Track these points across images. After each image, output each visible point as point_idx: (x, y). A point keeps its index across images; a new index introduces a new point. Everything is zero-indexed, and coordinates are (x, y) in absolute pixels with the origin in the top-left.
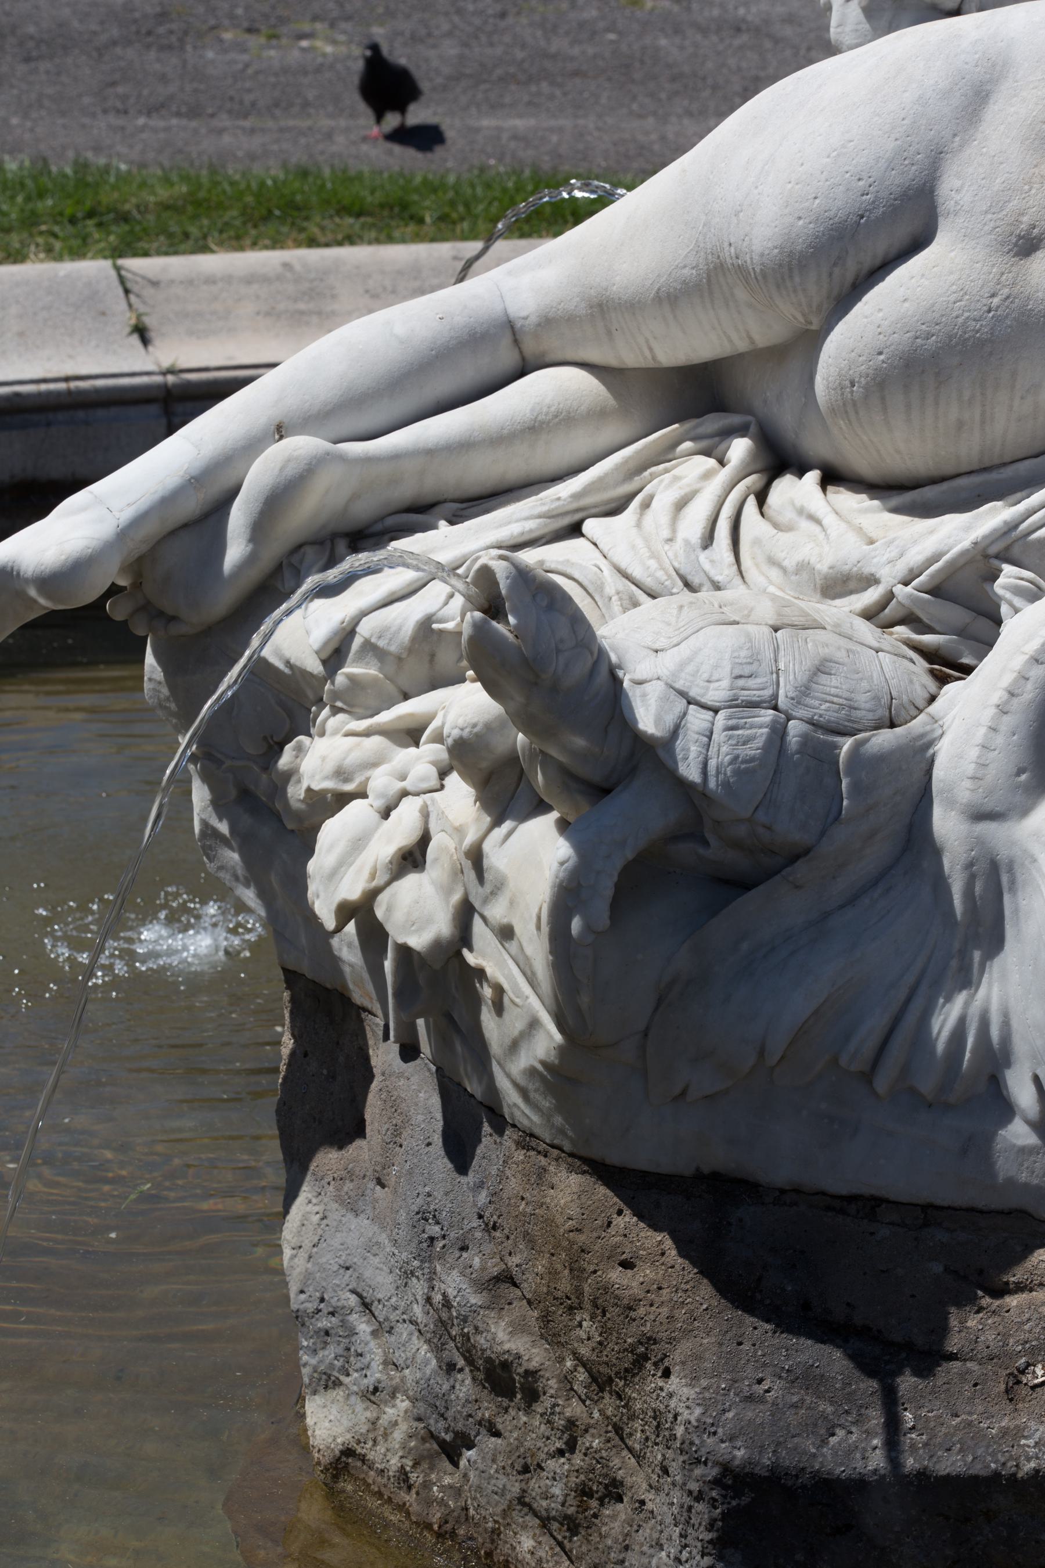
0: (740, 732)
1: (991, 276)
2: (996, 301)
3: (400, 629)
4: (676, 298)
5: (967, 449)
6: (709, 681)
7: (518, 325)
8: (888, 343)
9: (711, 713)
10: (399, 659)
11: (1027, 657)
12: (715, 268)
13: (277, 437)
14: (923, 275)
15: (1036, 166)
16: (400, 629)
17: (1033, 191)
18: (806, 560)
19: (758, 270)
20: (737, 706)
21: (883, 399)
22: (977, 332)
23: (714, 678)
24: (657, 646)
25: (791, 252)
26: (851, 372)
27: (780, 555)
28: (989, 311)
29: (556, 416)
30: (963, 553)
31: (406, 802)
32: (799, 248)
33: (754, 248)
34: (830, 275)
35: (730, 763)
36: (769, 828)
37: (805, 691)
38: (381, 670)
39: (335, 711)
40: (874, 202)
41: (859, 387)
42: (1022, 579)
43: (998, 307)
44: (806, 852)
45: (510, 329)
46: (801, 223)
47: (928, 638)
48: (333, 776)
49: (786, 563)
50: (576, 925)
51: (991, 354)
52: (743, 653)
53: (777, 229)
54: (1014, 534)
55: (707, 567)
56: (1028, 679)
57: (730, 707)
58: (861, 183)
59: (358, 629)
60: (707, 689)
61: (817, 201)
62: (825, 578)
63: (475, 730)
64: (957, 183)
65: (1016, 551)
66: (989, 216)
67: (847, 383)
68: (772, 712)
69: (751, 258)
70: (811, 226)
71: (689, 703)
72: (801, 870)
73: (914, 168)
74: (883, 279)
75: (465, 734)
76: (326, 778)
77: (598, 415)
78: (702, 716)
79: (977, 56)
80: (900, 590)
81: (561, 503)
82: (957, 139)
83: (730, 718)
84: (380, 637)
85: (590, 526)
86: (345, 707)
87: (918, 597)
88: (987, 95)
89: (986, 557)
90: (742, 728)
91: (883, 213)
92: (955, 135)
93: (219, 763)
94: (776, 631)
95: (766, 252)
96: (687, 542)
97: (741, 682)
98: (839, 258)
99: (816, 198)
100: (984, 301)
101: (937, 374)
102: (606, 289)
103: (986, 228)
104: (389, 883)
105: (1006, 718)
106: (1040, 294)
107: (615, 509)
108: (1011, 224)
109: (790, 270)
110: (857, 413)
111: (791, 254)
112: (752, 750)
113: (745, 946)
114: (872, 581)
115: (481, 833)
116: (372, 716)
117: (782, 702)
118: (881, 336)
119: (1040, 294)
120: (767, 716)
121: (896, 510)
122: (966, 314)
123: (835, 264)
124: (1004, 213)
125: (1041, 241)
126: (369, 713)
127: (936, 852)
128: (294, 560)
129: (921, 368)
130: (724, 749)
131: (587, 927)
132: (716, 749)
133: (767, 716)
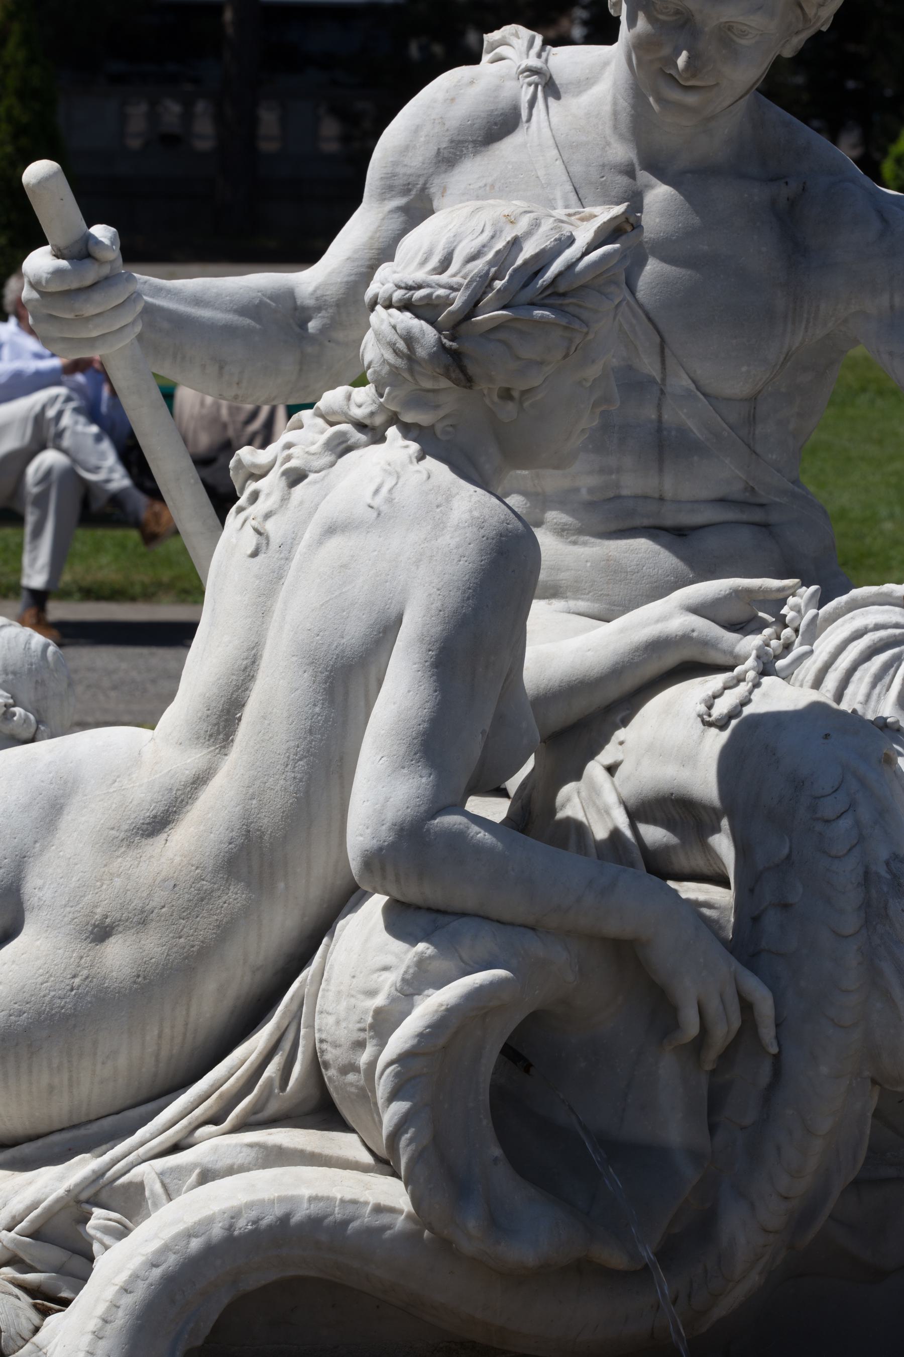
1: (72, 960)
2: (77, 981)
5: (58, 1109)
11: (117, 1287)
14: (14, 962)
15: (106, 865)
17: (104, 887)
22: (62, 1008)
28: (72, 990)
30: (58, 1200)
42: (110, 1220)
43: (79, 986)
47: (31, 1277)
51: (75, 1026)
54: (102, 1181)
56: (118, 1307)
64: (39, 882)
65: (104, 1196)
66: (68, 909)
79: (51, 775)
82: (38, 845)
88: (61, 808)
89: (79, 1202)
92: (36, 842)
100: (67, 982)
103: (66, 919)
105: (102, 1343)
106: (114, 974)
108: (87, 916)
119: (114, 974)
122: (52, 993)
124: (81, 906)
125: (113, 928)
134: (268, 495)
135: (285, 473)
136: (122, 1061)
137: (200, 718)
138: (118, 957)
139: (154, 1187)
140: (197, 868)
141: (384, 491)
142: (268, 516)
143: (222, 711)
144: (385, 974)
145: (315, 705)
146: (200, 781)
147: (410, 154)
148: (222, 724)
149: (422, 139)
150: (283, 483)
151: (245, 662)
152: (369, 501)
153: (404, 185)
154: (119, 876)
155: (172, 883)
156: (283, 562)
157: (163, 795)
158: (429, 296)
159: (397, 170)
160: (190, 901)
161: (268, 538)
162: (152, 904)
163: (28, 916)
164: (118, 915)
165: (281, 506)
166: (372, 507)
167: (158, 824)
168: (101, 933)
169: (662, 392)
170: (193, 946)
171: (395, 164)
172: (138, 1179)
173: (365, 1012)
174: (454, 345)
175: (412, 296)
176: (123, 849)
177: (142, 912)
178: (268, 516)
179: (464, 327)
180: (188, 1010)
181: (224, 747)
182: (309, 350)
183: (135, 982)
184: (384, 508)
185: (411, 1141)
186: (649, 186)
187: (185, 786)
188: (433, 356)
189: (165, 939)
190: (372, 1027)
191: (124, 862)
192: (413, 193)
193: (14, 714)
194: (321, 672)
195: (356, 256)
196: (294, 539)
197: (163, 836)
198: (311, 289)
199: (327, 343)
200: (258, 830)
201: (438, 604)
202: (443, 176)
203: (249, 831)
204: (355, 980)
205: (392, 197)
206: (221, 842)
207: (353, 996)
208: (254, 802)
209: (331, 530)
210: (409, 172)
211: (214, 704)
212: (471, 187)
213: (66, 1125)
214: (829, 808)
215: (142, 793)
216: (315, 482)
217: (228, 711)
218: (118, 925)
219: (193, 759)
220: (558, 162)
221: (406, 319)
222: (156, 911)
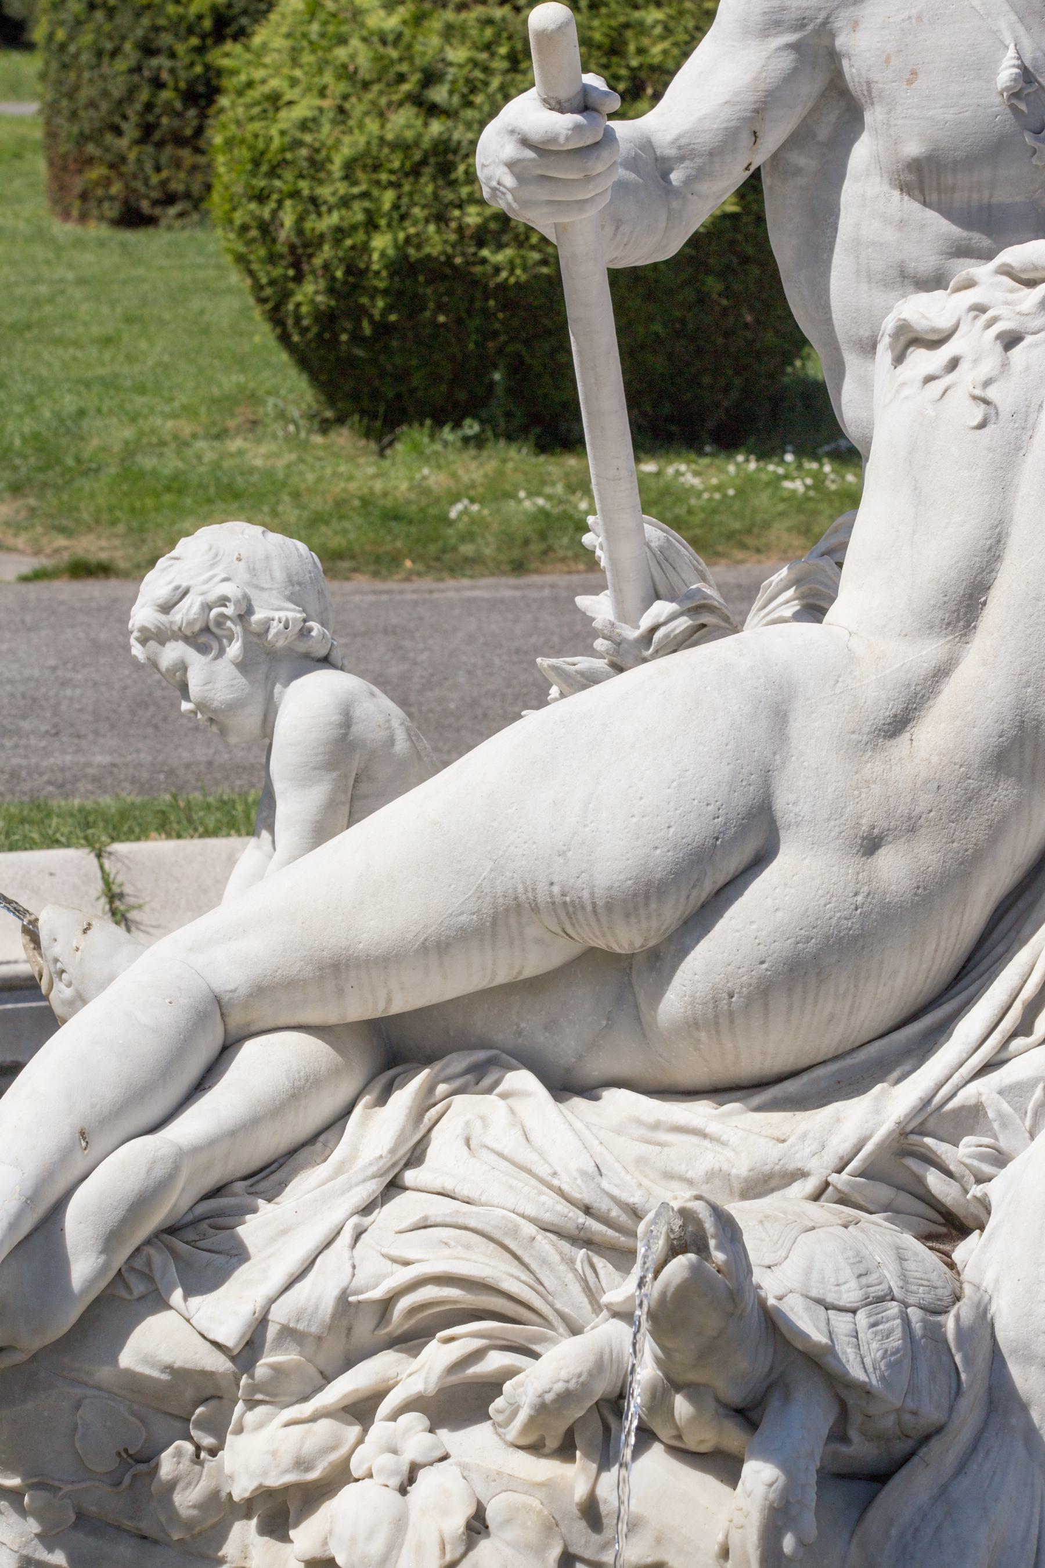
0: (880, 1327)
1: (850, 877)
2: (860, 899)
3: (317, 1308)
4: (448, 945)
5: (828, 1042)
6: (838, 1285)
7: (225, 998)
8: (771, 952)
9: (851, 1314)
10: (319, 1339)
12: (507, 910)
13: (84, 1144)
15: (856, 773)
16: (317, 1308)
17: (863, 796)
18: (717, 1168)
19: (600, 903)
20: (871, 1303)
21: (766, 1005)
22: (850, 929)
23: (841, 1281)
24: (767, 1263)
26: (729, 985)
27: (681, 1169)
28: (856, 909)
29: (307, 1080)
30: (890, 1134)
31: (422, 1475)
32: (658, 876)
33: (597, 883)
34: (688, 897)
35: (883, 1358)
36: (914, 1413)
37: (904, 1277)
38: (301, 1354)
39: (252, 1404)
40: (725, 824)
41: (740, 997)
42: (981, 1146)
43: (863, 904)
44: (939, 1430)
45: (219, 1005)
46: (658, 852)
48: (293, 1468)
49: (690, 1175)
50: (788, 1543)
51: (863, 948)
52: (850, 1254)
54: (929, 1109)
55: (615, 1192)
57: (867, 1305)
58: (710, 808)
59: (270, 1317)
60: (840, 1292)
61: (672, 830)
62: (746, 1181)
63: (582, 1379)
64: (792, 797)
65: (930, 1125)
66: (832, 823)
67: (725, 996)
68: (894, 1303)
69: (592, 894)
70: (670, 853)
71: (827, 1309)
72: (935, 1446)
73: (751, 788)
74: (741, 895)
75: (572, 1385)
76: (286, 1471)
77: (335, 1073)
78: (844, 1319)
79: (762, 681)
80: (834, 1178)
81: (384, 1160)
82: (777, 757)
83: (869, 1316)
84: (298, 1321)
85: (410, 1177)
86: (267, 1398)
87: (859, 1184)
88: (785, 715)
90: (882, 1323)
91: (735, 833)
92: (775, 754)
93: (54, 1490)
94: (846, 1227)
96: (583, 1173)
97: (864, 1280)
98: (698, 880)
101: (819, 974)
102: (347, 949)
103: (833, 834)
104: (464, 1555)
106: (893, 887)
107: (415, 1157)
109: (647, 897)
110: (732, 1021)
111: (649, 883)
112: (896, 1341)
113: (894, 1532)
114: (801, 1174)
115: (592, 1481)
116: (305, 1399)
117: (897, 1292)
118: (761, 947)
119: (893, 887)
120: (894, 1308)
121: (758, 1109)
123: (694, 887)
124: (844, 818)
125: (882, 839)
126: (294, 1399)
127: (1024, 1408)
128: (139, 1263)
129: (803, 969)
130: (874, 1345)
131: (801, 1543)
132: (866, 1347)
133: (894, 1308)
134: (976, 361)
135: (999, 337)
136: (900, 980)
137: (934, 606)
138: (895, 869)
139: (995, 1106)
140: (961, 766)
142: (987, 384)
143: (964, 595)
146: (941, 673)
148: (963, 610)
150: (999, 347)
151: (989, 542)
153: (797, 20)
154: (874, 782)
155: (936, 785)
156: (1019, 432)
161: (996, 408)
162: (918, 809)
163: (782, 833)
164: (885, 825)
165: (1002, 372)
167: (898, 724)
168: (871, 845)
170: (967, 850)
172: (972, 1101)
176: (869, 753)
177: (910, 818)
178: (987, 384)
180: (962, 919)
181: (965, 635)
182: (675, 204)
183: (915, 894)
187: (925, 680)
189: (940, 845)
191: (874, 767)
192: (810, 28)
193: (310, 630)
195: (737, 99)
197: (906, 736)
198: (670, 137)
199: (690, 196)
200: (1034, 720)
202: (852, 9)
203: (1023, 722)
206: (989, 736)
208: (1029, 690)
211: (952, 589)
212: (891, 20)
213: (830, 1056)
215: (874, 690)
216: (1036, 345)
217: (971, 596)
218: (887, 835)
219: (930, 651)
222: (924, 816)
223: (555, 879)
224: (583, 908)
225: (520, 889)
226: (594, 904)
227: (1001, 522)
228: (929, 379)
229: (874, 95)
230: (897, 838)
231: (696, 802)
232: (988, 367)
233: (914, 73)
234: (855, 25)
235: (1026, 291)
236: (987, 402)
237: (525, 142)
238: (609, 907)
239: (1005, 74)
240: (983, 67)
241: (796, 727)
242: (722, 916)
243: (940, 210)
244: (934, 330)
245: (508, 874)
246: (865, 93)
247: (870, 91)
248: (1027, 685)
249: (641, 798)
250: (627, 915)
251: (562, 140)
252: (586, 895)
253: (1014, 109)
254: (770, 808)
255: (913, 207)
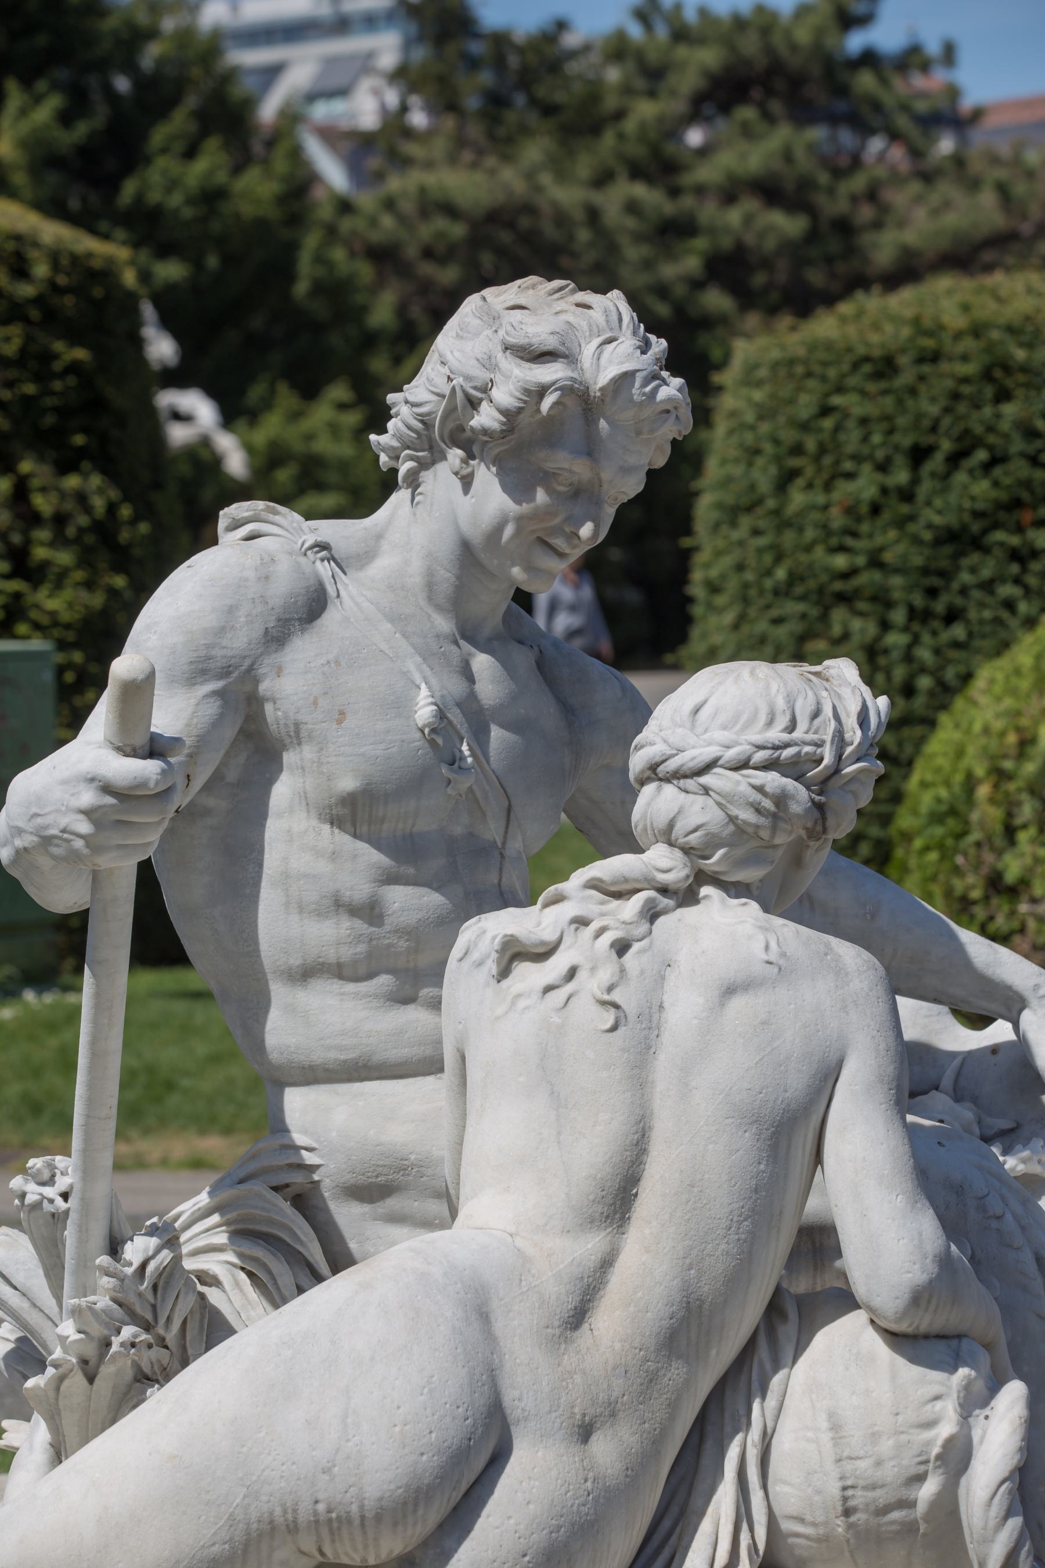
8: (531, 1544)
12: (260, 1535)
17: (570, 1386)
25: (418, 1487)
32: (426, 1481)
33: (367, 1495)
46: (425, 1458)
51: (598, 1532)
53: (399, 1471)
58: (460, 1410)
61: (434, 1435)
64: (516, 1393)
66: (554, 1415)
69: (362, 1507)
70: (435, 1458)
74: (492, 1492)
88: (487, 1316)
95: (388, 1494)
99: (431, 1432)
106: (609, 1471)
108: (571, 1417)
111: (418, 1490)
118: (522, 1540)
122: (577, 1502)
123: (454, 1489)
134: (593, 969)
137: (593, 1201)
138: (608, 1451)
140: (641, 1350)
141: (773, 945)
142: (610, 989)
143: (619, 1189)
144: (938, 1405)
145: (759, 1163)
146: (607, 1263)
147: (229, 636)
149: (243, 619)
150: (614, 956)
152: (766, 958)
153: (223, 668)
155: (623, 1370)
156: (646, 1032)
157: (575, 1285)
158: (799, 753)
159: (213, 653)
160: (642, 1384)
162: (615, 1394)
163: (513, 1429)
165: (621, 978)
166: (770, 963)
167: (578, 1317)
168: (585, 1432)
169: (502, 856)
171: (209, 646)
173: (929, 1443)
174: (823, 799)
175: (780, 755)
176: (563, 1346)
177: (610, 1404)
178: (610, 989)
179: (833, 780)
181: (621, 1226)
183: (627, 1476)
184: (781, 962)
185: (1029, 1552)
186: (474, 655)
188: (807, 811)
189: (635, 1427)
190: (939, 1457)
191: (569, 1360)
194: (767, 1129)
196: (651, 1008)
197: (585, 1326)
200: (698, 1300)
201: (883, 1046)
202: (274, 656)
203: (689, 1303)
204: (900, 1418)
205: (206, 680)
206: (661, 1320)
207: (902, 1432)
208: (692, 1272)
209: (730, 990)
210: (230, 654)
212: (312, 665)
214: (995, 1206)
217: (625, 1189)
220: (397, 635)
221: (773, 780)
223: (321, 1496)
224: (350, 1522)
225: (278, 1511)
226: (363, 1518)
227: (643, 1117)
228: (548, 989)
229: (301, 735)
230: (603, 1423)
231: (448, 1406)
232: (606, 974)
233: (342, 713)
234: (279, 671)
235: (615, 903)
236: (616, 1006)
237: (107, 788)
238: (378, 1518)
239: (424, 712)
240: (402, 705)
241: (499, 1326)
242: (479, 1516)
243: (369, 841)
244: (543, 943)
245: (264, 1498)
246: (292, 734)
247: (297, 732)
248: (690, 1268)
249: (399, 1407)
250: (395, 1524)
251: (152, 784)
252: (354, 1508)
253: (432, 743)
254: (501, 1405)
255: (344, 839)
